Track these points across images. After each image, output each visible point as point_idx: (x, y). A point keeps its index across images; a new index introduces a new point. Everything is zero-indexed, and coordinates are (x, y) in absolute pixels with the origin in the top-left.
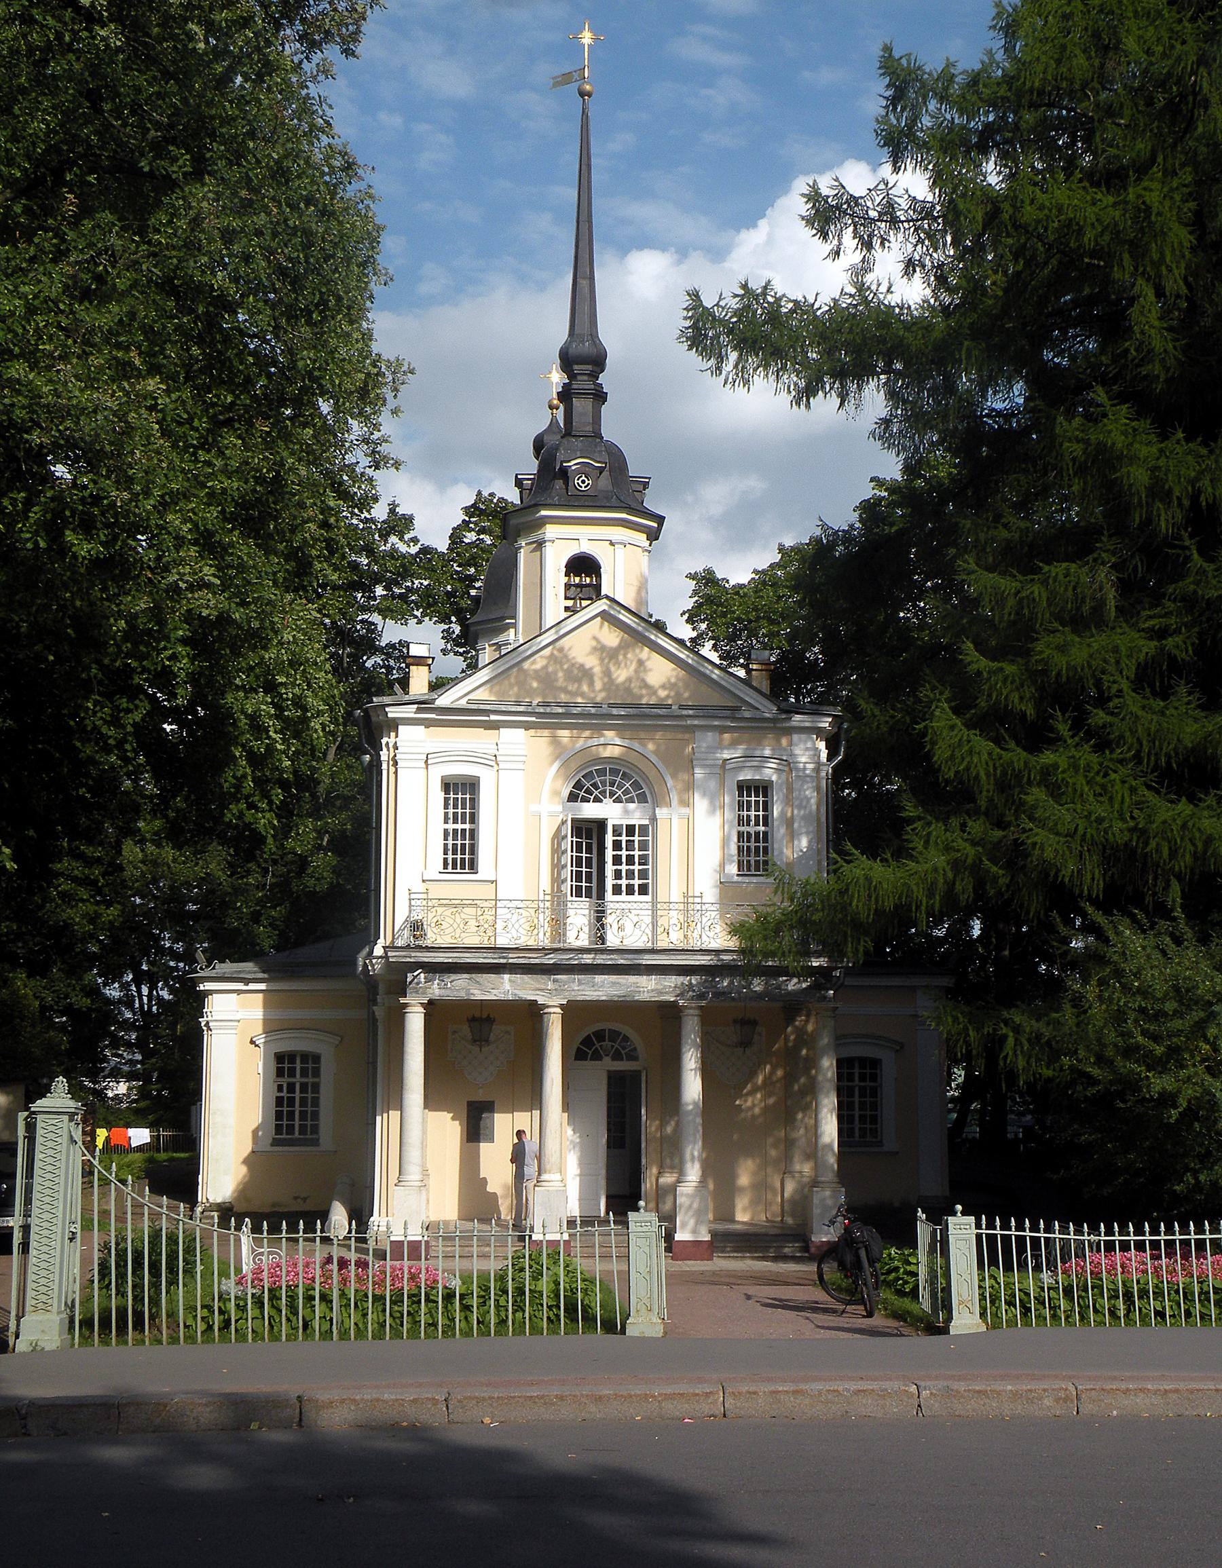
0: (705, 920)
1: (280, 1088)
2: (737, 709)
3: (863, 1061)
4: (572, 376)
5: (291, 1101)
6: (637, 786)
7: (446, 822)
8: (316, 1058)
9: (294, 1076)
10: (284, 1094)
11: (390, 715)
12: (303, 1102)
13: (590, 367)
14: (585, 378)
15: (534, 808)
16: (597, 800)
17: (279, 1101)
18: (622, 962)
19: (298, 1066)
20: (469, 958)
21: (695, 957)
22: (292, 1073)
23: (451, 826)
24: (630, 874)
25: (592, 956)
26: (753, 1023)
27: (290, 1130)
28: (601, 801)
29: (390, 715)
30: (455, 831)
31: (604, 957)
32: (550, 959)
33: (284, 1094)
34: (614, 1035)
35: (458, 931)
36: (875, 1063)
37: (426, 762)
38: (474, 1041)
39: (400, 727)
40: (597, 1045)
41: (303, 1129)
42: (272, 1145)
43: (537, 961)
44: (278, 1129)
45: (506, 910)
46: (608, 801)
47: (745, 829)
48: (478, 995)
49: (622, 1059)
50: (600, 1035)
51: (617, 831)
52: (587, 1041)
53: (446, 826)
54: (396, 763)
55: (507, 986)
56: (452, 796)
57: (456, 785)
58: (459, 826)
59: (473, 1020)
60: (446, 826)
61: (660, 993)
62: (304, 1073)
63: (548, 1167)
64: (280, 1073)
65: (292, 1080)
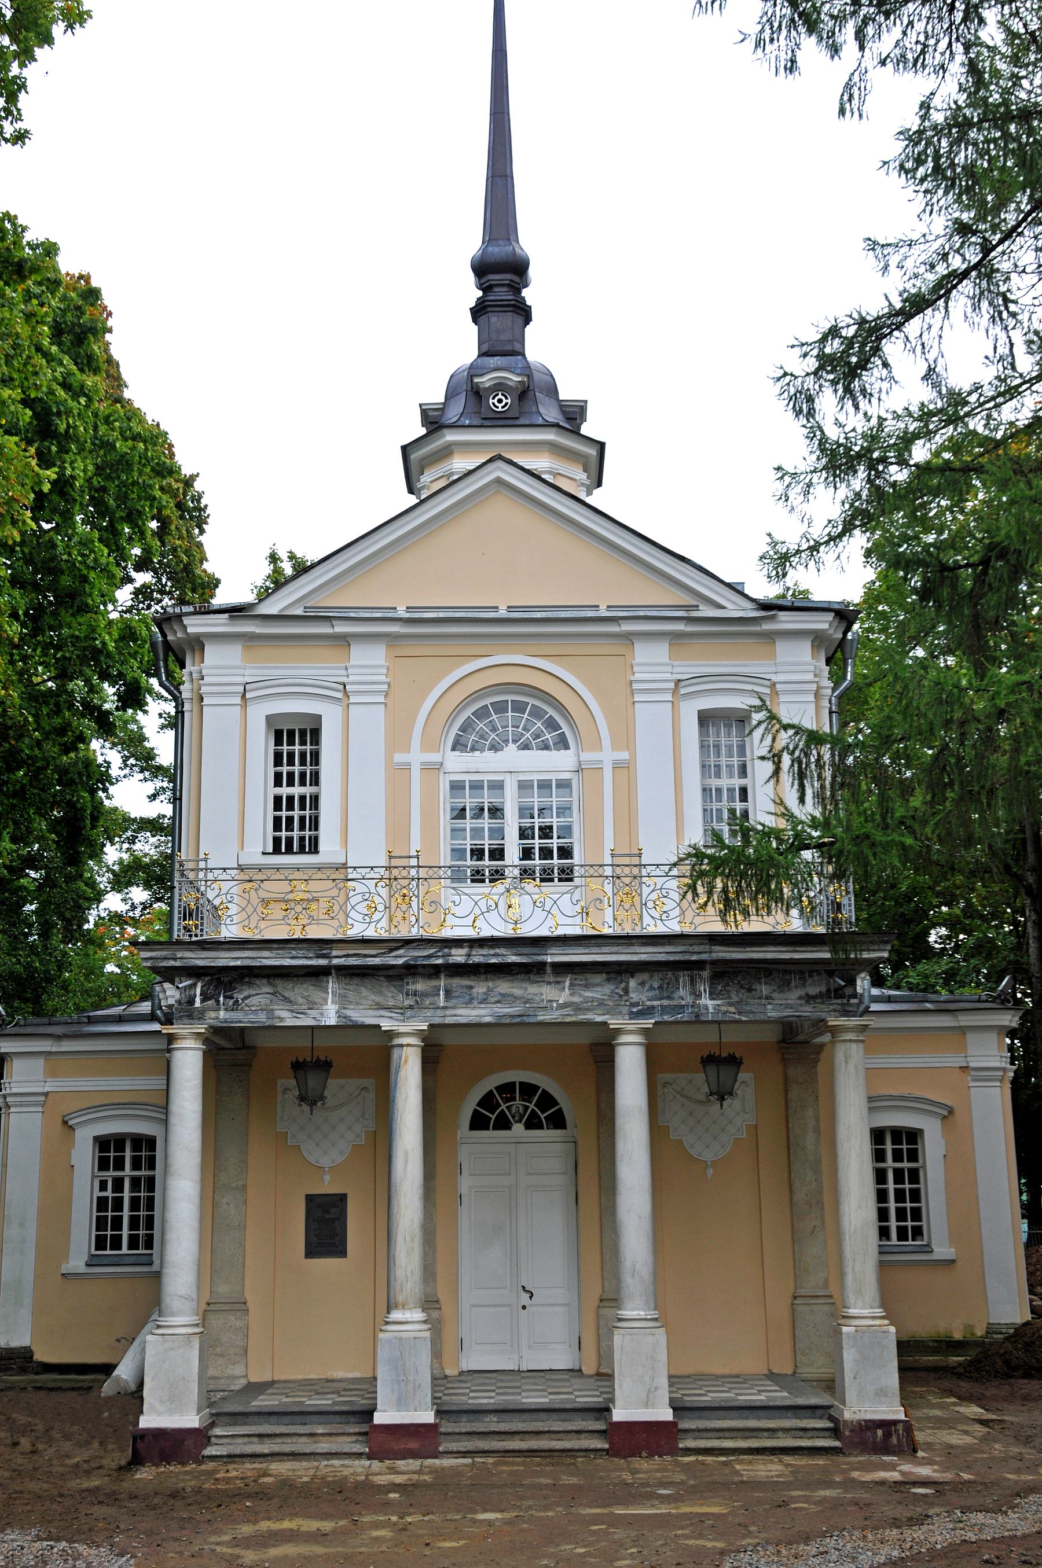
0: (646, 891)
1: (103, 1186)
3: (896, 1133)
4: (486, 289)
5: (118, 1204)
6: (552, 725)
7: (278, 783)
9: (123, 1169)
10: (109, 1193)
11: (190, 630)
12: (135, 1203)
13: (509, 276)
14: (505, 289)
15: (399, 758)
16: (495, 748)
17: (102, 1204)
18: (514, 959)
19: (128, 1154)
21: (632, 949)
22: (119, 1165)
23: (285, 791)
24: (546, 853)
25: (464, 951)
26: (734, 1062)
27: (116, 1244)
29: (190, 630)
30: (290, 799)
31: (485, 951)
32: (399, 958)
33: (109, 1193)
34: (528, 1090)
35: (254, 918)
36: (914, 1136)
37: (244, 696)
38: (302, 1098)
39: (208, 649)
40: (503, 1107)
41: (133, 1243)
42: (88, 1265)
43: (377, 961)
44: (100, 1243)
45: (331, 884)
46: (512, 747)
49: (541, 1127)
50: (506, 1089)
52: (488, 1101)
53: (278, 791)
56: (285, 748)
57: (291, 733)
58: (297, 790)
59: (298, 1066)
60: (278, 791)
61: (578, 1008)
62: (136, 1165)
63: (400, 1298)
64: (103, 1164)
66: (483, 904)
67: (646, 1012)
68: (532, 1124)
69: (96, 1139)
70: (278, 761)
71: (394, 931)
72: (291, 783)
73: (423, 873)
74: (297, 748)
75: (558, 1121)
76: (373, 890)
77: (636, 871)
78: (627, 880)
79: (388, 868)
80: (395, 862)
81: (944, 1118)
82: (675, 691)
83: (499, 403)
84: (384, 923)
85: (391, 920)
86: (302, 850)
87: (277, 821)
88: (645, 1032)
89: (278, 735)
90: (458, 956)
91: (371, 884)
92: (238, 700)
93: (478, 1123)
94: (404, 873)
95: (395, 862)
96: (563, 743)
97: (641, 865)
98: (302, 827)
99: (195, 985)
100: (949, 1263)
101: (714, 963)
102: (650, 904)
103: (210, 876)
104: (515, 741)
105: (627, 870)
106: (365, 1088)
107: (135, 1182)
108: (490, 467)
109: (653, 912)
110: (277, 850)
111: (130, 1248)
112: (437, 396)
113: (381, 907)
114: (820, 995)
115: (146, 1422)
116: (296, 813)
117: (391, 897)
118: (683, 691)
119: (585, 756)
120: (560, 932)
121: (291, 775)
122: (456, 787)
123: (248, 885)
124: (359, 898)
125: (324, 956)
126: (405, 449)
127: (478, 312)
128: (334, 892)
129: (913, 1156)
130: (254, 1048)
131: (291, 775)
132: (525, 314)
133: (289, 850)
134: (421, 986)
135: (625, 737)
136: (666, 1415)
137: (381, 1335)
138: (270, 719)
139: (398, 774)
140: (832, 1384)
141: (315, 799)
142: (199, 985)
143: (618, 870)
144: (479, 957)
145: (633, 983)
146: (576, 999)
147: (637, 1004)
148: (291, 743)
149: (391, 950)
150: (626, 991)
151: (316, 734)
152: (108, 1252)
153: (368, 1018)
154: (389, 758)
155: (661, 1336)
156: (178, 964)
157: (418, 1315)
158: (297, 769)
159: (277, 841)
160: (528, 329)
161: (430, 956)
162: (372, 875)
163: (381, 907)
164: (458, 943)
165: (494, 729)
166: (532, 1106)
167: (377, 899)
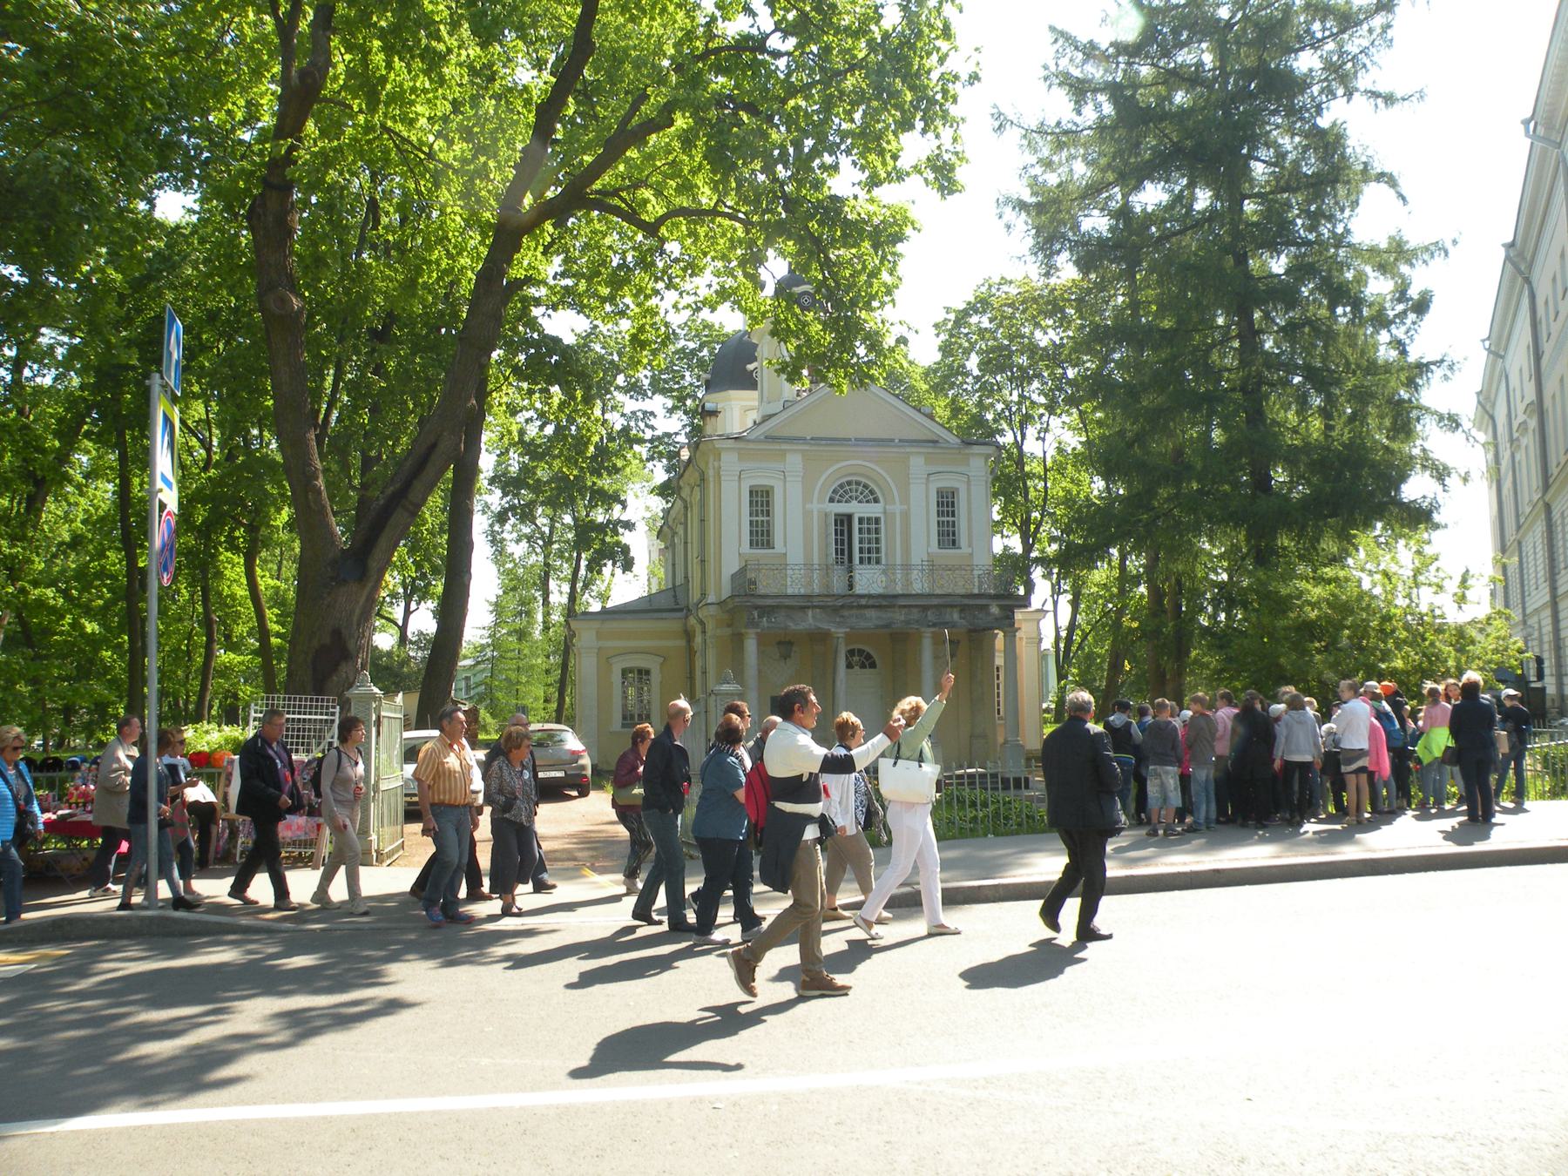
2: (937, 442)
8: (648, 672)
20: (787, 602)
32: (840, 603)
46: (854, 502)
47: (941, 519)
48: (792, 626)
51: (861, 520)
55: (811, 620)
67: (934, 625)
82: (927, 479)
90: (863, 602)
96: (876, 500)
134: (846, 613)
135: (906, 499)
139: (807, 515)
144: (871, 602)
153: (825, 626)
154: (804, 507)
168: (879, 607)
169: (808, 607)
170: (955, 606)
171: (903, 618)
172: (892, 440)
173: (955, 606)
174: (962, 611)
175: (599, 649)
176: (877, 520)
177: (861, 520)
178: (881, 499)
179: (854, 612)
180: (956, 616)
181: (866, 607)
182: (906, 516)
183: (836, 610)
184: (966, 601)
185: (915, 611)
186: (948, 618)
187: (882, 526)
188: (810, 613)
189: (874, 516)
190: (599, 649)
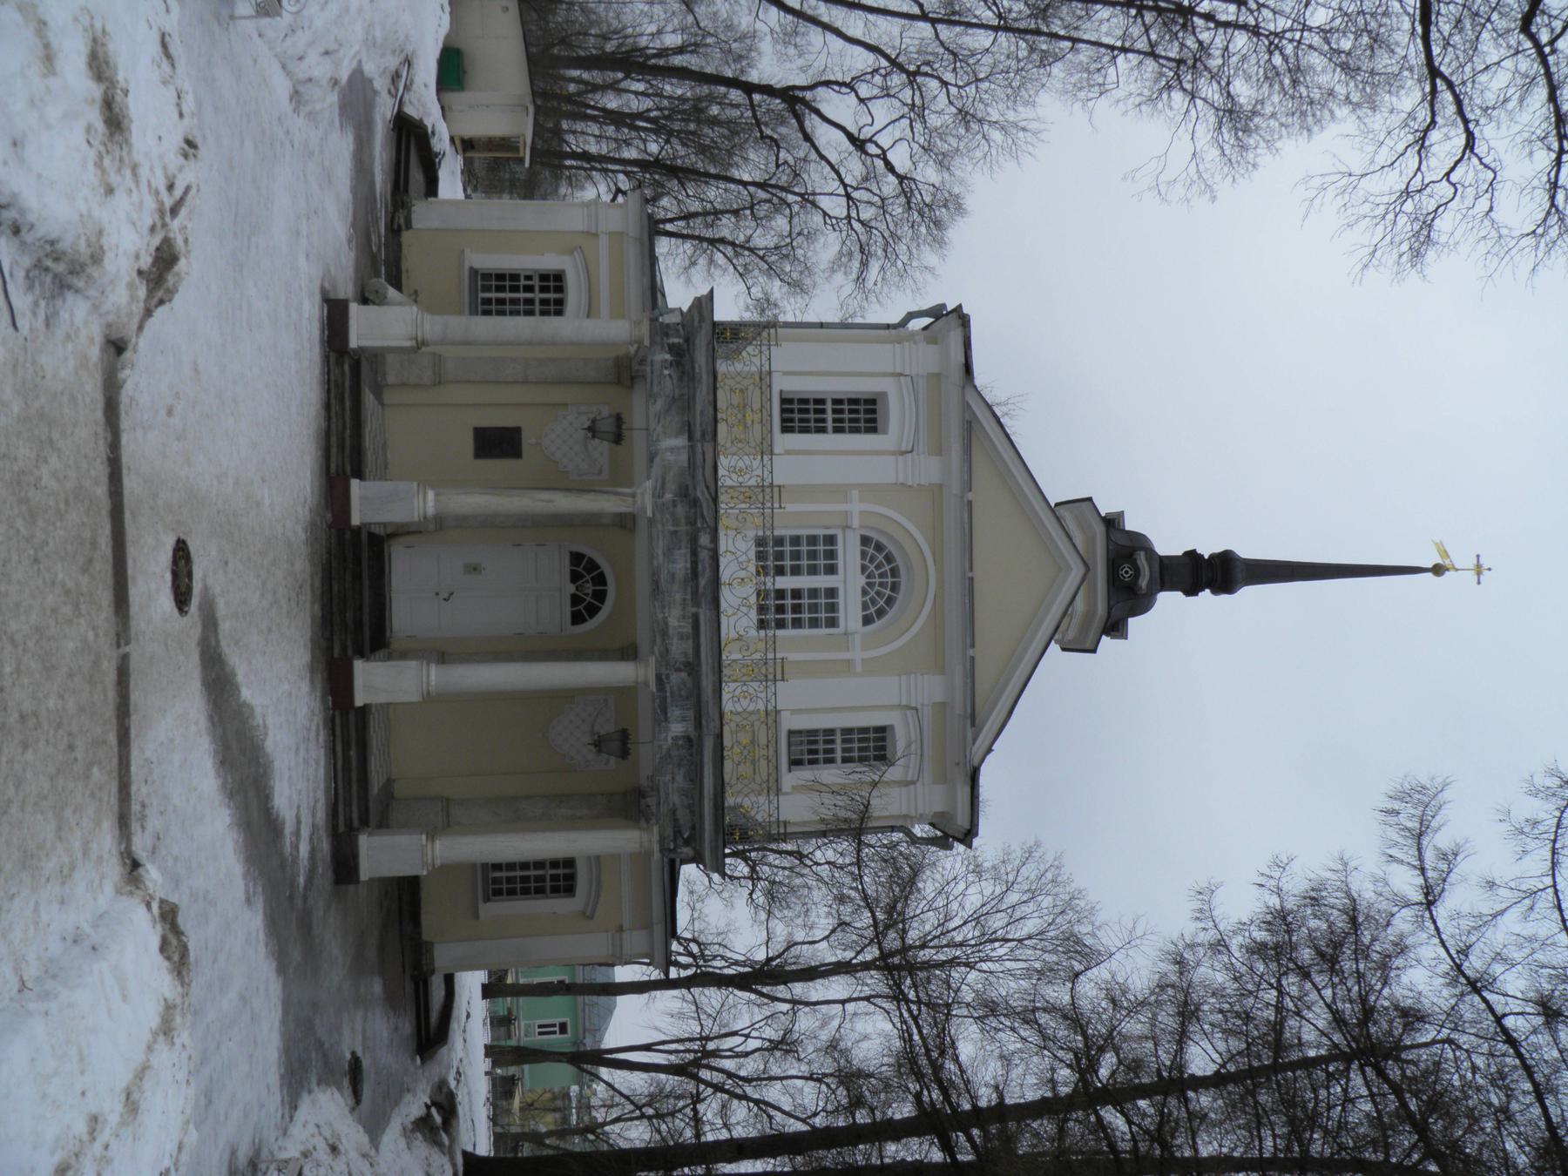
0: (755, 685)
1: (528, 278)
5: (515, 289)
7: (836, 402)
10: (523, 282)
11: (952, 333)
16: (864, 568)
17: (515, 277)
22: (544, 289)
26: (624, 753)
27: (486, 289)
28: (863, 572)
30: (823, 411)
32: (701, 494)
34: (601, 596)
36: (570, 890)
37: (901, 375)
40: (588, 577)
41: (487, 301)
43: (700, 477)
44: (487, 276)
46: (862, 580)
50: (601, 580)
51: (832, 593)
52: (592, 566)
54: (899, 343)
58: (829, 416)
59: (619, 419)
62: (544, 302)
64: (544, 277)
65: (537, 289)
66: (743, 558)
68: (576, 600)
69: (564, 271)
70: (853, 401)
71: (723, 490)
72: (835, 411)
73: (768, 511)
74: (862, 416)
75: (577, 619)
76: (755, 473)
77: (771, 677)
78: (763, 670)
79: (771, 485)
80: (776, 490)
81: (583, 913)
82: (908, 707)
83: (1126, 572)
84: (729, 483)
85: (731, 487)
86: (784, 420)
87: (806, 401)
88: (646, 684)
89: (873, 402)
90: (704, 540)
91: (759, 472)
92: (898, 370)
93: (577, 558)
94: (767, 497)
95: (776, 490)
96: (867, 620)
97: (775, 680)
98: (801, 420)
99: (680, 337)
100: (477, 916)
101: (700, 738)
102: (745, 688)
103: (764, 348)
104: (868, 584)
105: (771, 670)
106: (600, 472)
107: (529, 302)
108: (1079, 562)
109: (739, 690)
110: (784, 401)
111: (483, 299)
112: (1129, 526)
113: (741, 479)
114: (676, 820)
115: (354, 308)
116: (812, 416)
117: (749, 487)
118: (908, 712)
119: (857, 638)
120: (723, 619)
121: (841, 411)
122: (831, 540)
123: (757, 378)
124: (748, 463)
125: (703, 435)
126: (1090, 499)
127: (1192, 555)
128: (753, 444)
129: (555, 890)
130: (631, 387)
131: (841, 411)
132: (1191, 591)
133: (783, 411)
134: (681, 510)
136: (359, 702)
137: (415, 484)
138: (884, 395)
139: (840, 492)
140: (384, 824)
141: (823, 430)
142: (681, 341)
143: (771, 663)
144: (704, 555)
145: (684, 675)
146: (671, 632)
147: (668, 677)
148: (867, 411)
149: (707, 488)
150: (678, 670)
151: (874, 430)
152: (479, 283)
155: (414, 697)
156: (696, 323)
157: (431, 511)
158: (846, 416)
159: (790, 401)
160: (1180, 594)
161: (703, 516)
162: (766, 473)
163: (741, 479)
164: (715, 539)
165: (877, 567)
166: (589, 599)
167: (747, 476)
168: (695, 573)
169: (690, 439)
170: (698, 725)
171: (673, 622)
172: (973, 646)
173: (698, 725)
174: (688, 740)
175: (596, 235)
176: (832, 623)
177: (832, 593)
178: (870, 628)
179: (683, 528)
180: (677, 728)
181: (694, 553)
182: (847, 667)
183: (684, 493)
184: (709, 744)
185: (688, 646)
186: (675, 712)
187: (823, 631)
188: (681, 441)
189: (841, 615)
190: (596, 235)
